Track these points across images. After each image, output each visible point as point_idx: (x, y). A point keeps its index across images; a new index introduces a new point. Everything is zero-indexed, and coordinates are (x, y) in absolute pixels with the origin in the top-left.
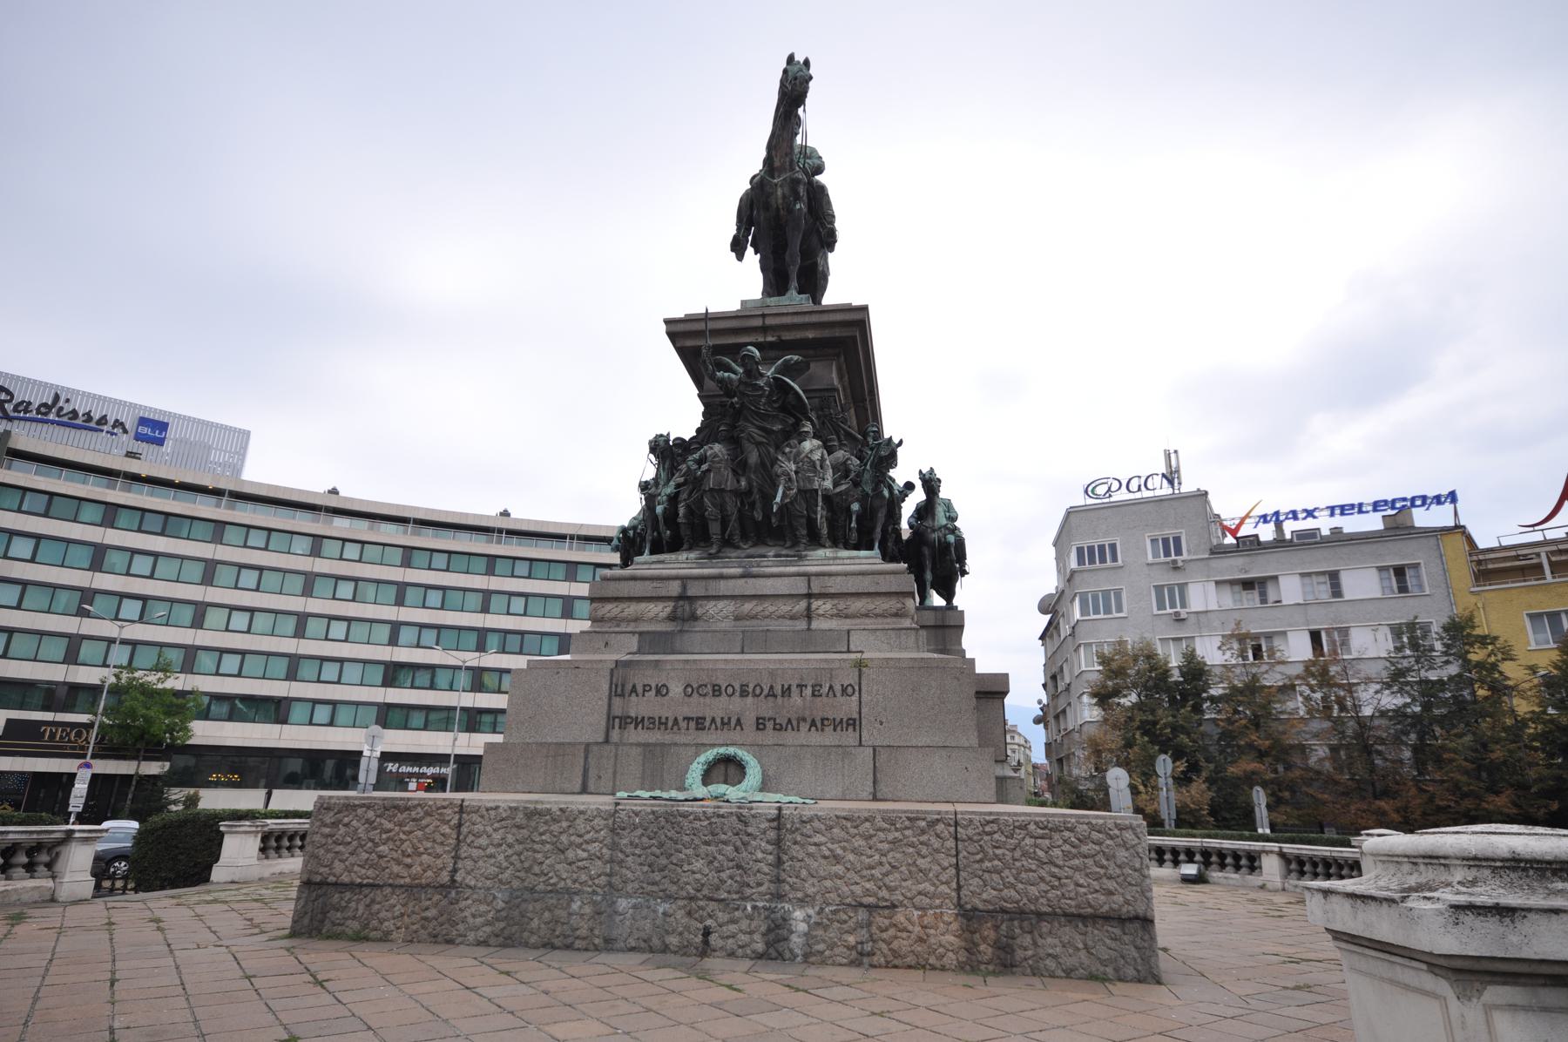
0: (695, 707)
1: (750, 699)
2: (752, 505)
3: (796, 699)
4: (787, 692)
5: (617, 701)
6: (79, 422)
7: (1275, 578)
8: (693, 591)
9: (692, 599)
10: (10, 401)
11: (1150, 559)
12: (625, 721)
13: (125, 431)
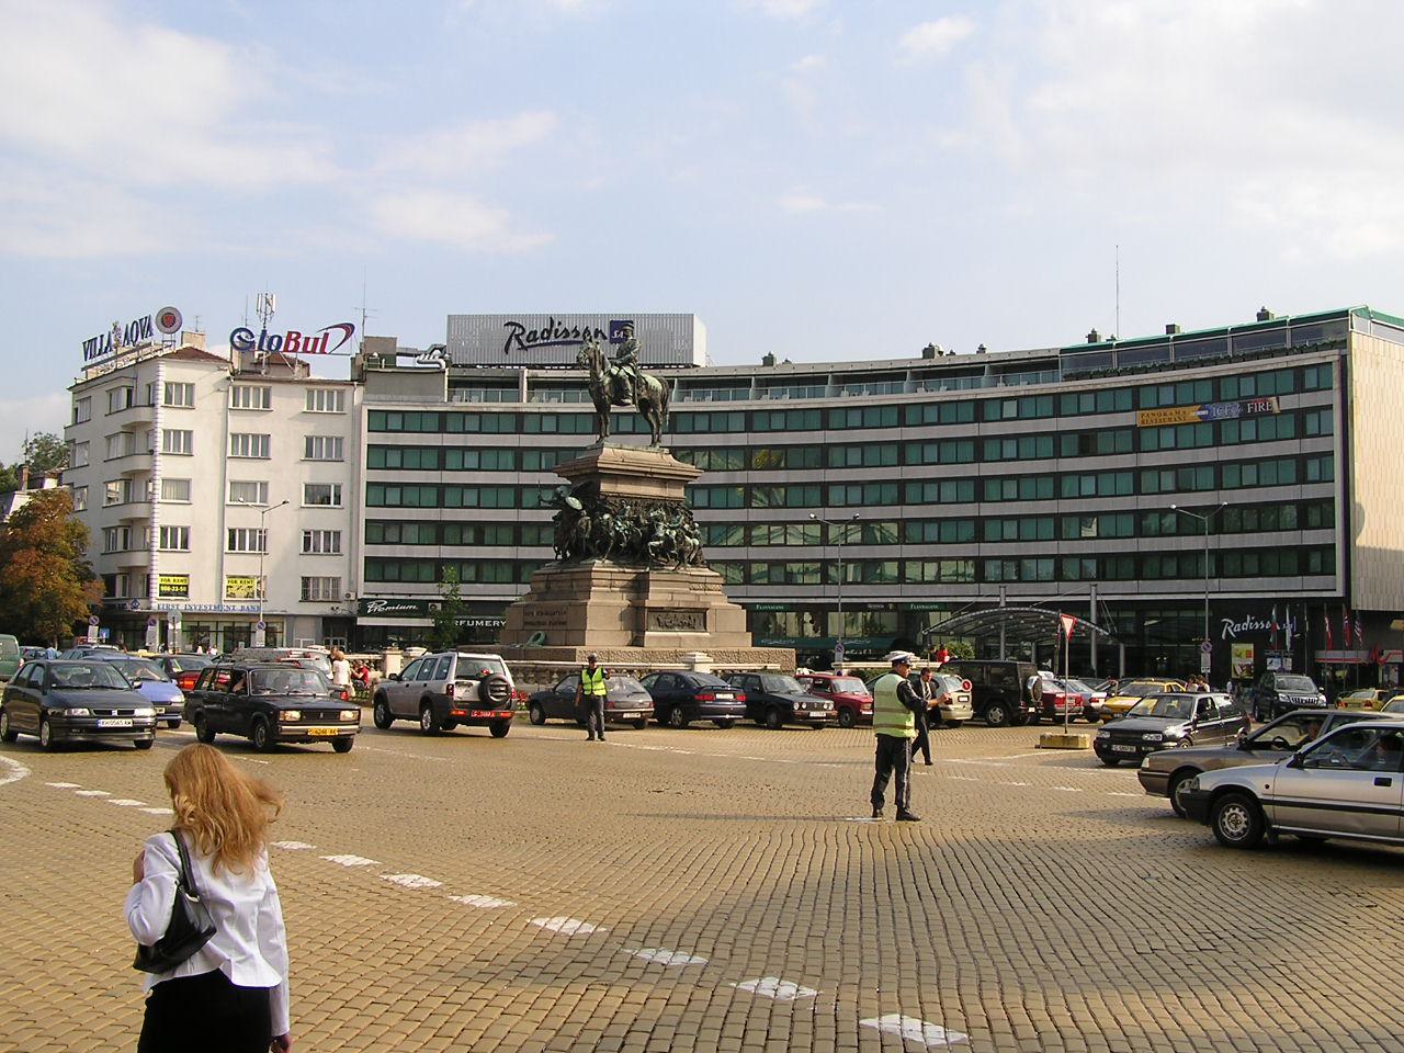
6: (571, 338)
10: (522, 333)
12: (526, 623)
13: (605, 338)
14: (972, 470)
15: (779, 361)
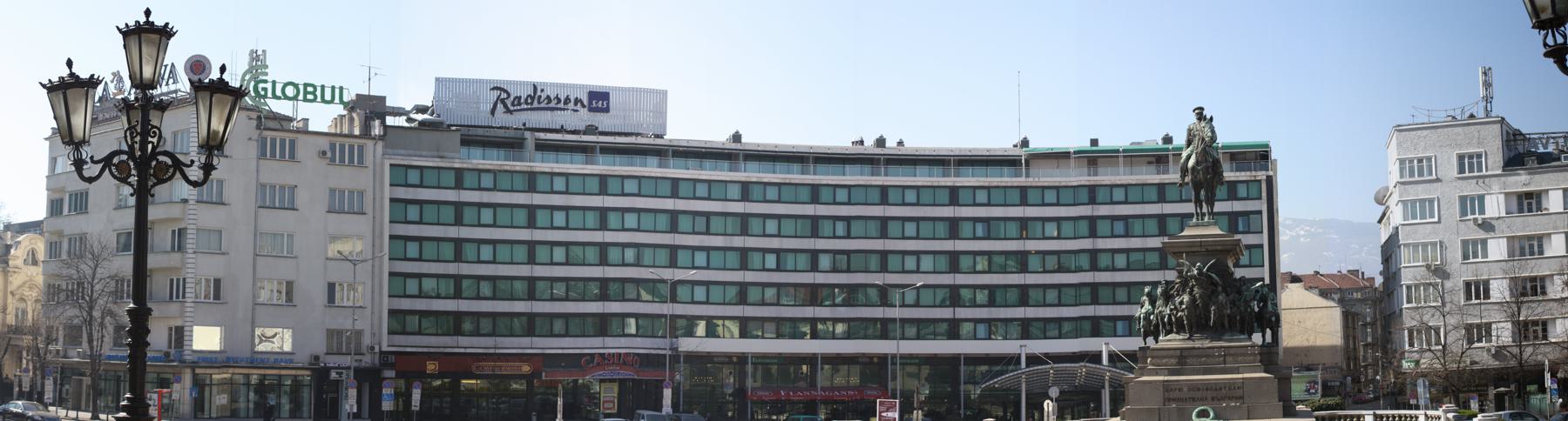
0: (1192, 394)
1: (1209, 392)
2: (1201, 318)
3: (1224, 391)
4: (1221, 389)
5: (1166, 394)
7: (1547, 191)
8: (1185, 353)
9: (1185, 357)
11: (1455, 174)
12: (1169, 400)
14: (948, 245)
15: (907, 144)
